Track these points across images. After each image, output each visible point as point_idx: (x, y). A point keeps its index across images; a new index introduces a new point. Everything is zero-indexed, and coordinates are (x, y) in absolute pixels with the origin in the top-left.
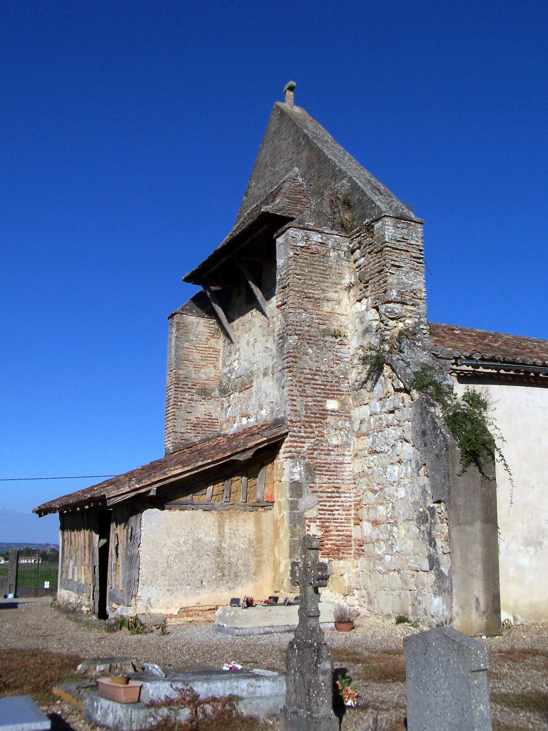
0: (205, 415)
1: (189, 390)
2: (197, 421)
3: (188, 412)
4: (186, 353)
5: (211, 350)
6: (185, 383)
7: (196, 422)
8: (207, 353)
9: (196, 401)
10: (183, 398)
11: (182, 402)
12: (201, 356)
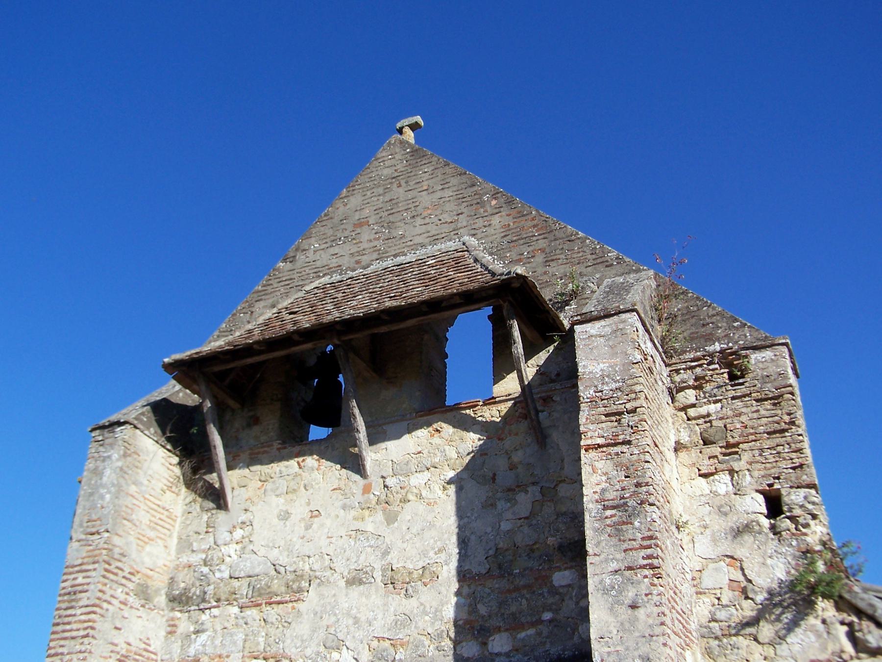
0: (141, 640)
1: (124, 581)
2: (127, 651)
3: (116, 628)
4: (130, 506)
5: (166, 513)
6: (119, 564)
7: (124, 652)
8: (158, 516)
9: (131, 607)
10: (112, 596)
11: (109, 603)
12: (150, 521)
